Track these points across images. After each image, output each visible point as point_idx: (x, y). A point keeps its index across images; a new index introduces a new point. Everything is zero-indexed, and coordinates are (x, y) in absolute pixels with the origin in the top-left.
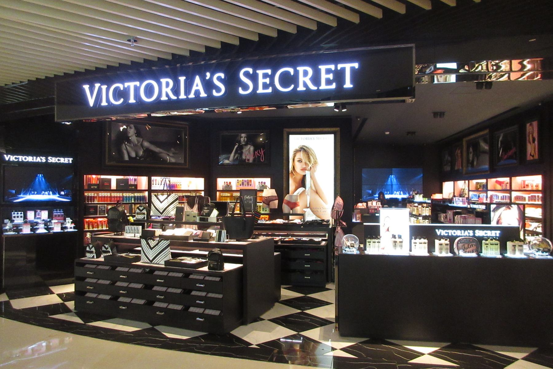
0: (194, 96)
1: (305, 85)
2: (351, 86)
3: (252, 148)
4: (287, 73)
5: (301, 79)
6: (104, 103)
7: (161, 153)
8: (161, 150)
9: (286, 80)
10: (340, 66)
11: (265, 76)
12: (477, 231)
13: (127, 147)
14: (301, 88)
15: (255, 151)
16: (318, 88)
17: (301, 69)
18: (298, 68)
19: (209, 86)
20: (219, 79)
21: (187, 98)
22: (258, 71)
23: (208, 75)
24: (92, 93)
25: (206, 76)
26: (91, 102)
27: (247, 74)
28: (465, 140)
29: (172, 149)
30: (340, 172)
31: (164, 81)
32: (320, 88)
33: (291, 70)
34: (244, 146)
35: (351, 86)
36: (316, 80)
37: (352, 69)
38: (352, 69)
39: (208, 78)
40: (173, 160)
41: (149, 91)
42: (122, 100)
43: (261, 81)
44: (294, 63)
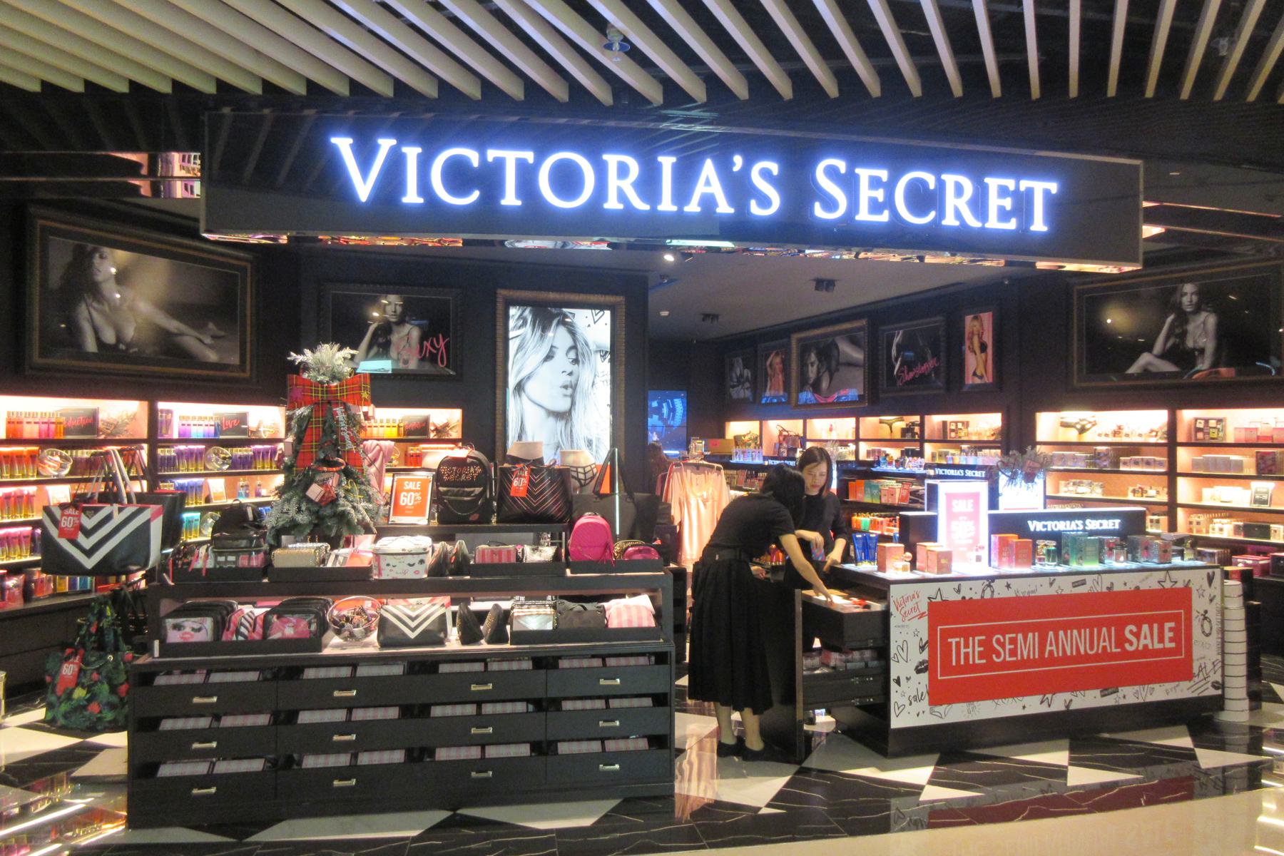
0: (698, 209)
1: (622, 197)
2: (1044, 229)
3: (415, 333)
4: (923, 183)
5: (951, 201)
6: (412, 197)
7: (182, 334)
8: (183, 327)
9: (923, 199)
10: (1025, 184)
11: (875, 183)
12: (1088, 521)
13: (95, 314)
14: (950, 221)
15: (423, 338)
16: (654, 208)
17: (950, 179)
18: (944, 177)
19: (739, 188)
20: (766, 174)
21: (681, 210)
22: (858, 171)
23: (738, 161)
24: (365, 165)
25: (733, 164)
26: (363, 189)
27: (832, 173)
28: (795, 337)
29: (211, 325)
30: (627, 400)
31: (612, 160)
32: (987, 225)
33: (930, 179)
34: (395, 328)
35: (1044, 229)
36: (979, 203)
37: (1047, 193)
38: (1047, 193)
39: (736, 169)
40: (212, 357)
41: (566, 180)
42: (475, 195)
43: (865, 193)
44: (939, 161)
